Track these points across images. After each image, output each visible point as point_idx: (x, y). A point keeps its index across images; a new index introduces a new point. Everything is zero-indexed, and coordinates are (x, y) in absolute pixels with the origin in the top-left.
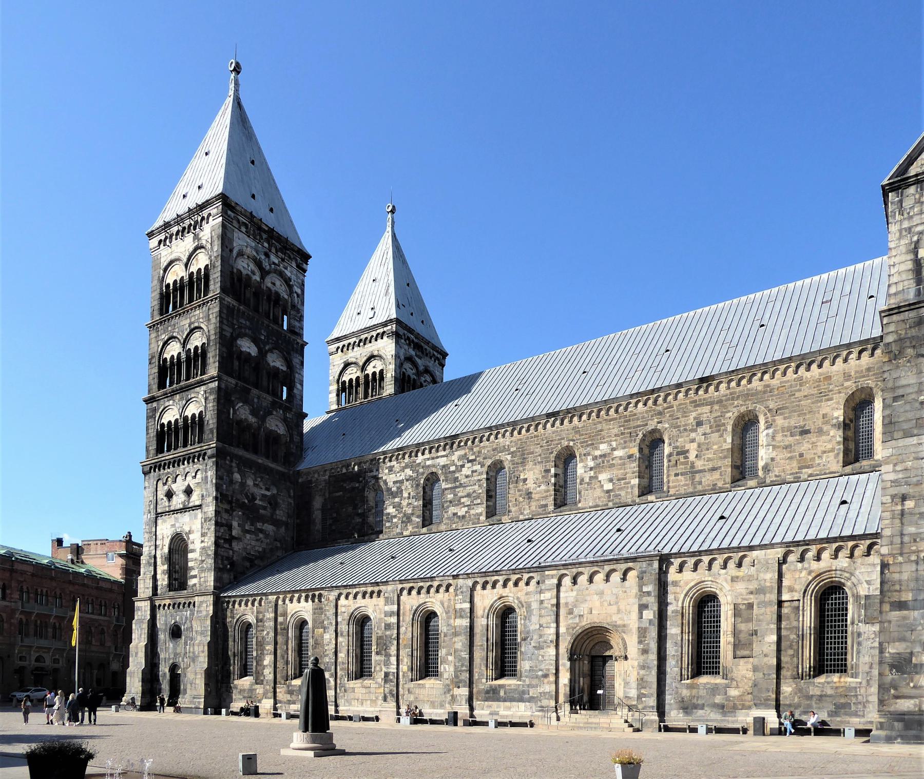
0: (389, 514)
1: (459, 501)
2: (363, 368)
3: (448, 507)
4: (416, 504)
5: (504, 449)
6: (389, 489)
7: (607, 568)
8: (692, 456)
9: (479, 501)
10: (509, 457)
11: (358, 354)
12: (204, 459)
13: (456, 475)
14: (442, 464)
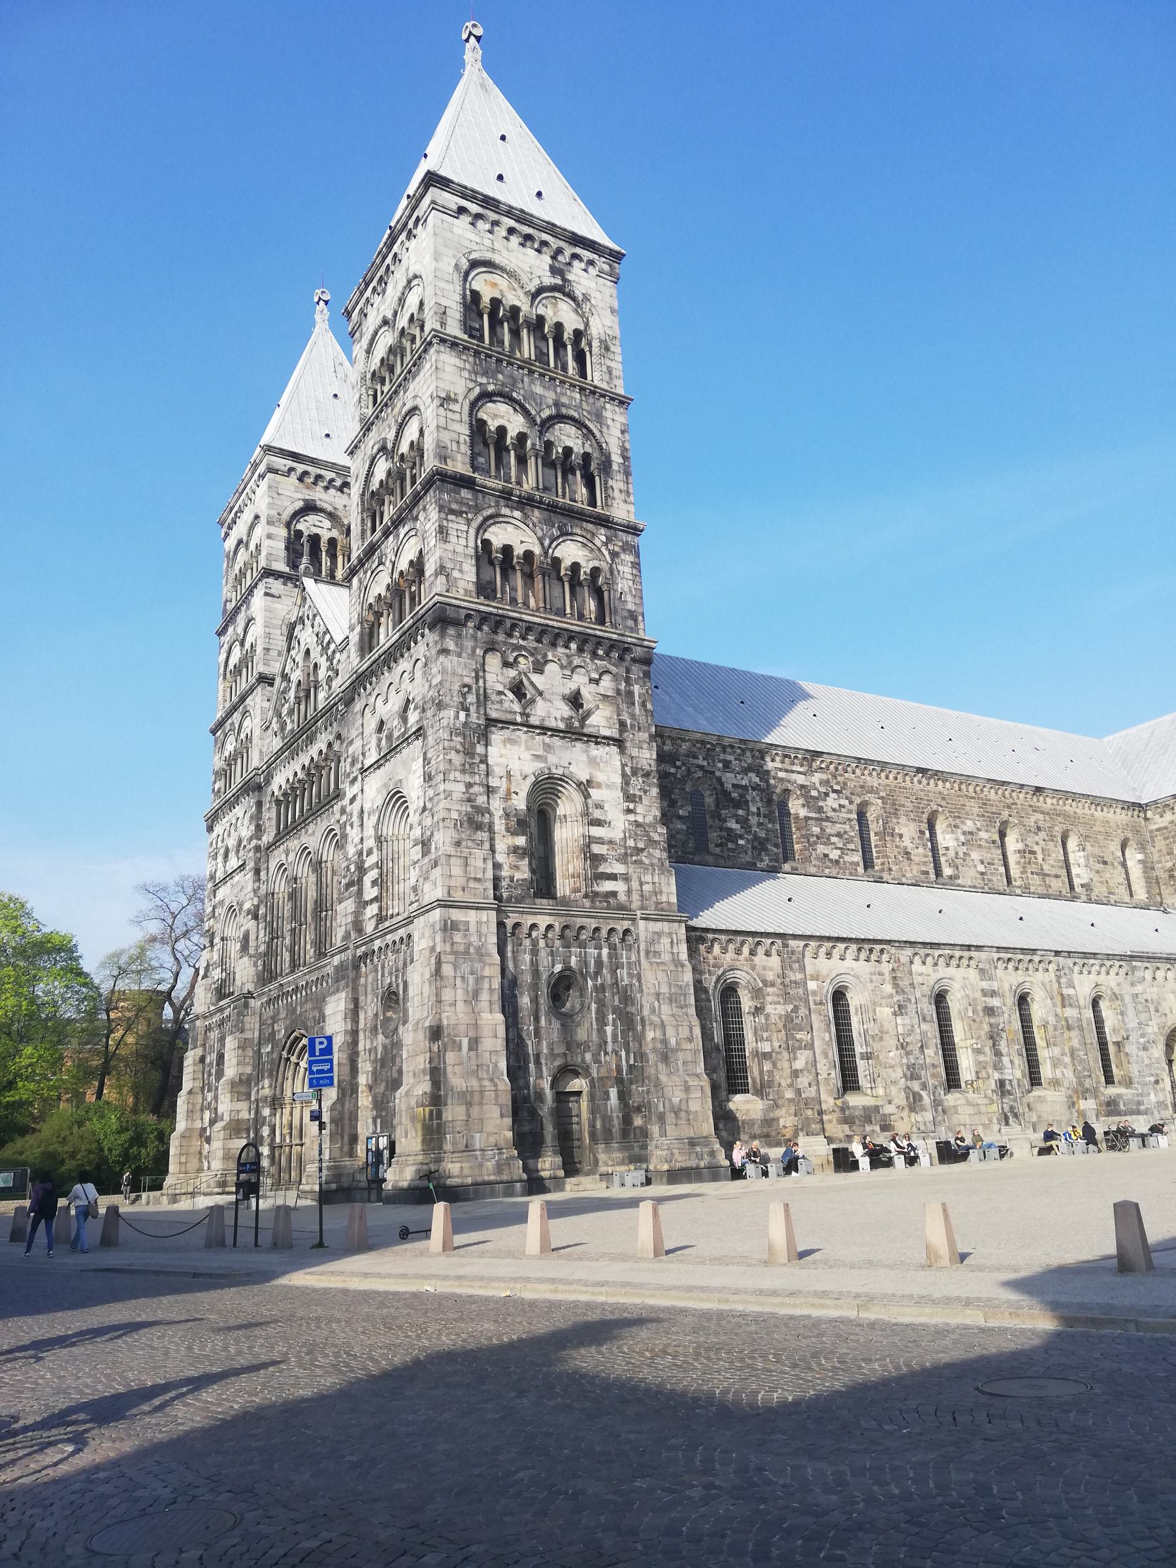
0: (731, 830)
1: (828, 839)
3: (815, 843)
4: (770, 826)
6: (726, 794)
8: (1040, 856)
9: (852, 846)
10: (880, 802)
12: (621, 658)
13: (820, 804)
14: (800, 782)
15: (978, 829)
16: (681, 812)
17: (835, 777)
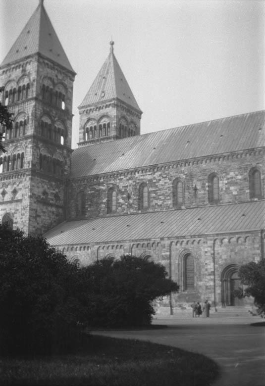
0: (120, 203)
2: (99, 121)
4: (135, 198)
5: (182, 172)
7: (237, 236)
10: (184, 176)
11: (96, 114)
14: (149, 178)
15: (237, 175)
16: (104, 201)
17: (164, 172)
